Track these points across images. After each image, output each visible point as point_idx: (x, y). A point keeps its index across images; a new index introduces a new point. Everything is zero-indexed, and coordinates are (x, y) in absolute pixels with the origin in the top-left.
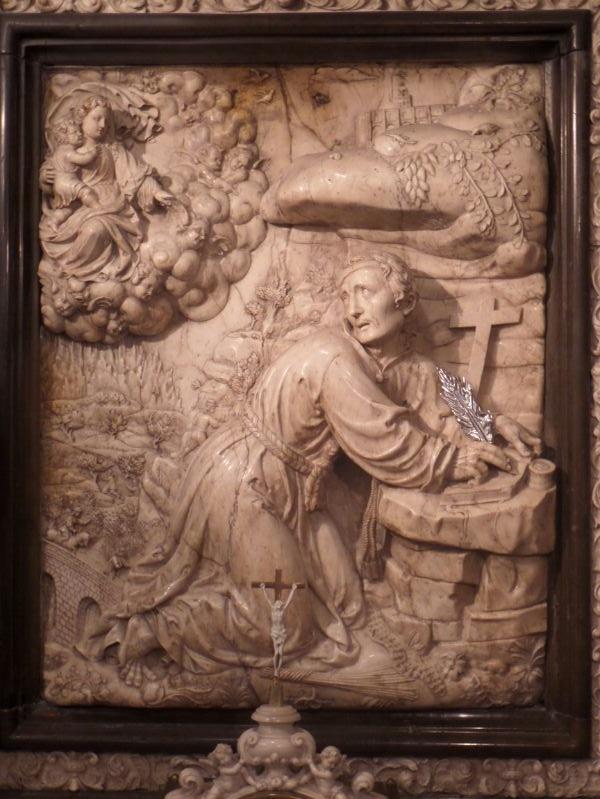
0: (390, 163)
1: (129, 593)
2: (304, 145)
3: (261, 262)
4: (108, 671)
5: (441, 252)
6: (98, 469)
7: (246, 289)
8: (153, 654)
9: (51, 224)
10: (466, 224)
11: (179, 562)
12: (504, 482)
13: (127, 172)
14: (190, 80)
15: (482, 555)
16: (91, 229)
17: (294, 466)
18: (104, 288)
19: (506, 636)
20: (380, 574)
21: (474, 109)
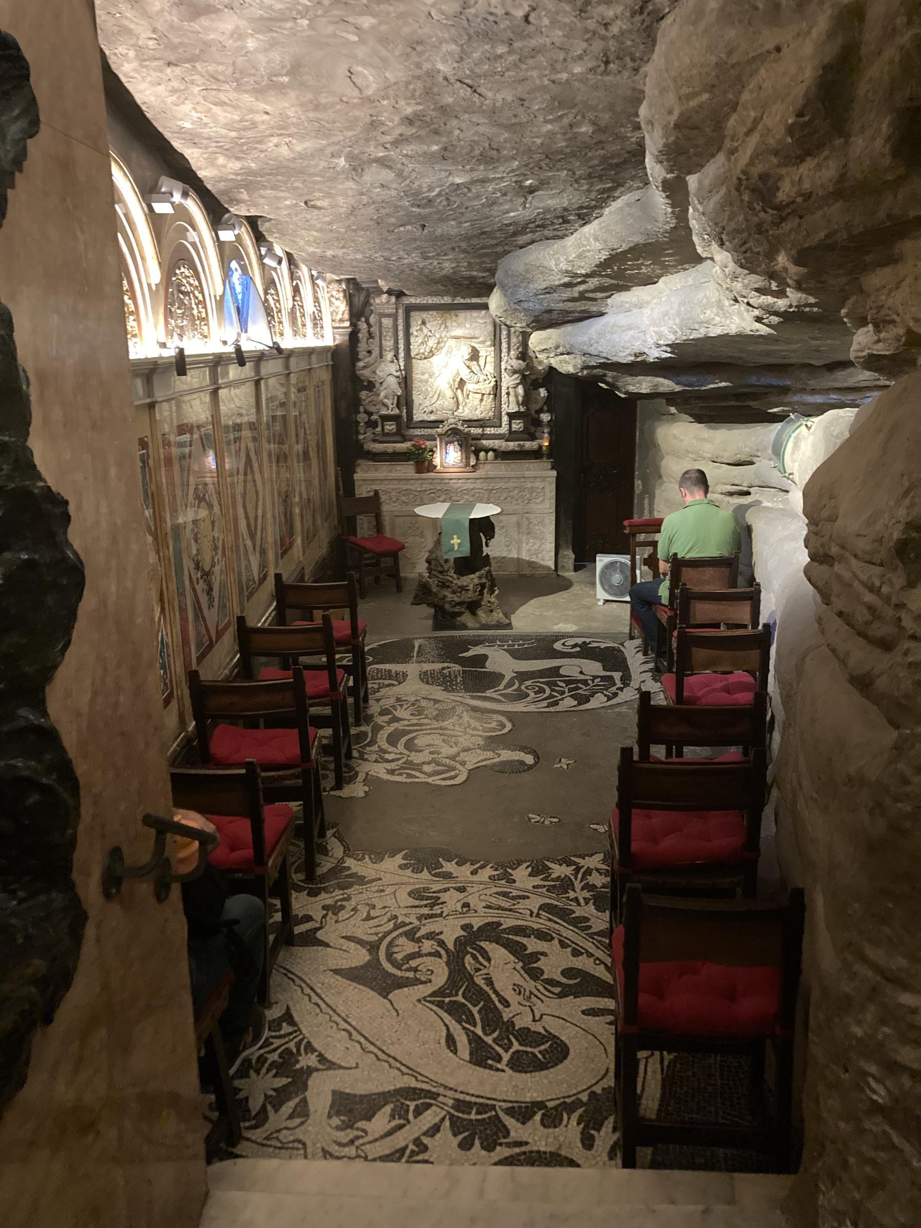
0: (468, 329)
1: (427, 403)
2: (454, 324)
3: (448, 344)
4: (425, 415)
5: (479, 343)
6: (421, 381)
7: (445, 350)
8: (432, 412)
9: (412, 340)
10: (481, 339)
11: (436, 396)
12: (487, 382)
13: (425, 331)
14: (434, 313)
15: (483, 394)
16: (420, 341)
17: (454, 381)
18: (422, 351)
19: (488, 407)
20: (468, 398)
21: (482, 318)
